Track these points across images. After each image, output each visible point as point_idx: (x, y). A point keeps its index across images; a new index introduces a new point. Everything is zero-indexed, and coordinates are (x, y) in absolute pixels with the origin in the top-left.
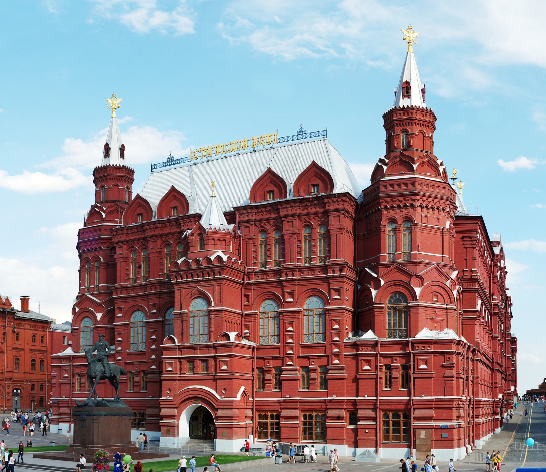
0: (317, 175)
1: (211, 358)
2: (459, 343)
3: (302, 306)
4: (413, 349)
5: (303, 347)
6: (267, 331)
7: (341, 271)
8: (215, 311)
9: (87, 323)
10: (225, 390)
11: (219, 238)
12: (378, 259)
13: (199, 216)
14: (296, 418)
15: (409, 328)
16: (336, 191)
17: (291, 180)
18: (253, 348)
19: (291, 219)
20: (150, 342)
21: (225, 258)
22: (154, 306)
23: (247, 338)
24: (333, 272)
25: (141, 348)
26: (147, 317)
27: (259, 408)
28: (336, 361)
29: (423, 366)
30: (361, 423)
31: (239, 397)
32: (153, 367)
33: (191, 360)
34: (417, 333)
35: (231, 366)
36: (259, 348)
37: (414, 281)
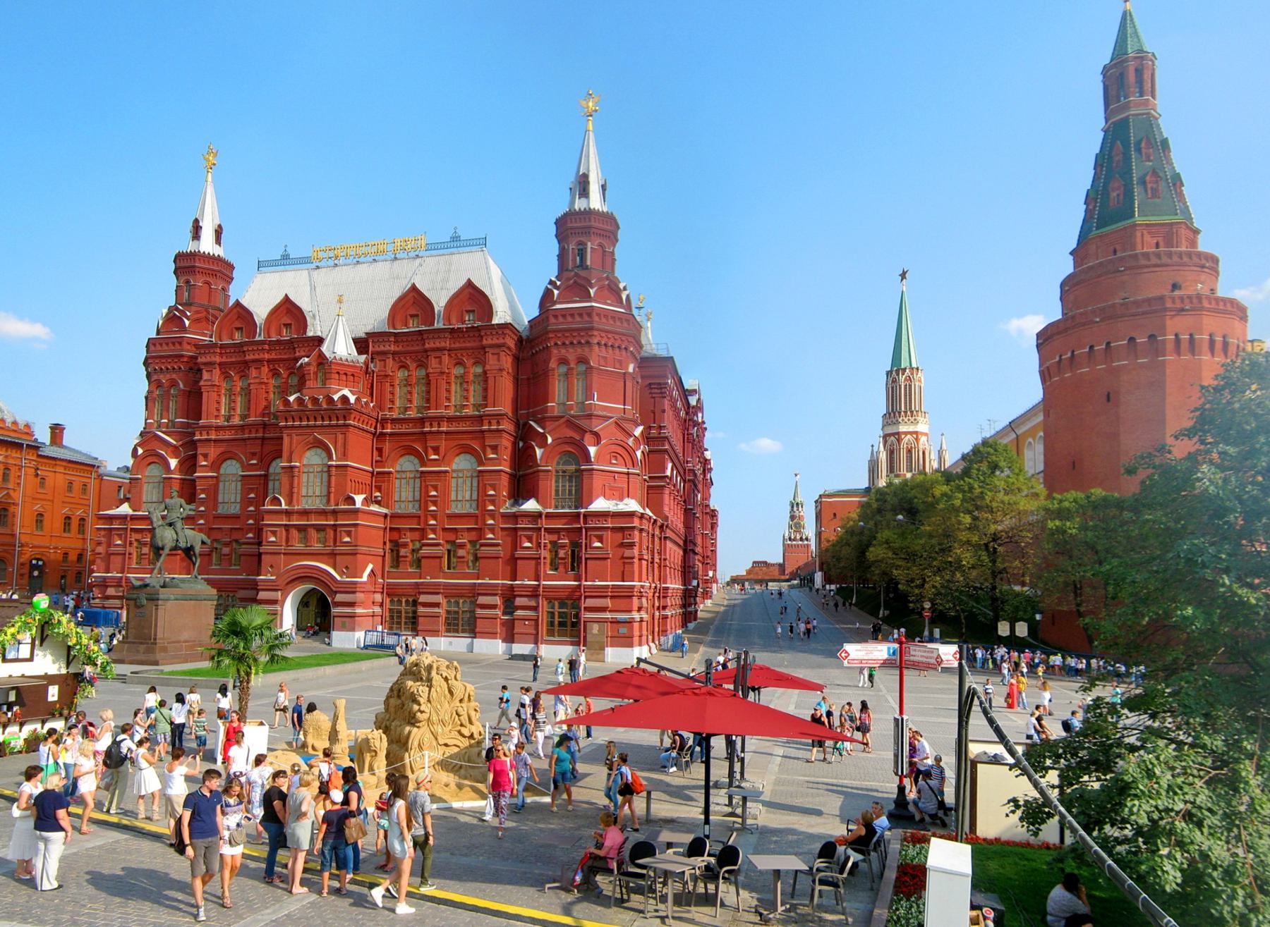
0: (473, 298)
1: (332, 527)
2: (642, 516)
3: (449, 465)
4: (585, 523)
5: (450, 516)
6: (405, 496)
7: (498, 423)
8: (337, 466)
9: (154, 471)
10: (347, 568)
11: (345, 372)
12: (546, 410)
13: (320, 340)
14: (437, 605)
15: (581, 498)
16: (495, 321)
17: (440, 301)
18: (386, 516)
19: (438, 354)
20: (246, 502)
21: (352, 399)
22: (254, 454)
23: (378, 503)
24: (490, 423)
25: (235, 509)
26: (244, 468)
27: (392, 592)
28: (491, 536)
29: (598, 544)
30: (519, 613)
31: (365, 578)
32: (250, 535)
33: (302, 529)
34: (591, 502)
35: (356, 538)
36: (393, 516)
37: (588, 437)
